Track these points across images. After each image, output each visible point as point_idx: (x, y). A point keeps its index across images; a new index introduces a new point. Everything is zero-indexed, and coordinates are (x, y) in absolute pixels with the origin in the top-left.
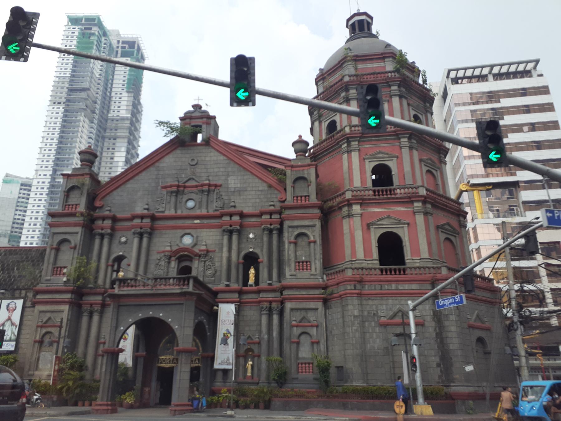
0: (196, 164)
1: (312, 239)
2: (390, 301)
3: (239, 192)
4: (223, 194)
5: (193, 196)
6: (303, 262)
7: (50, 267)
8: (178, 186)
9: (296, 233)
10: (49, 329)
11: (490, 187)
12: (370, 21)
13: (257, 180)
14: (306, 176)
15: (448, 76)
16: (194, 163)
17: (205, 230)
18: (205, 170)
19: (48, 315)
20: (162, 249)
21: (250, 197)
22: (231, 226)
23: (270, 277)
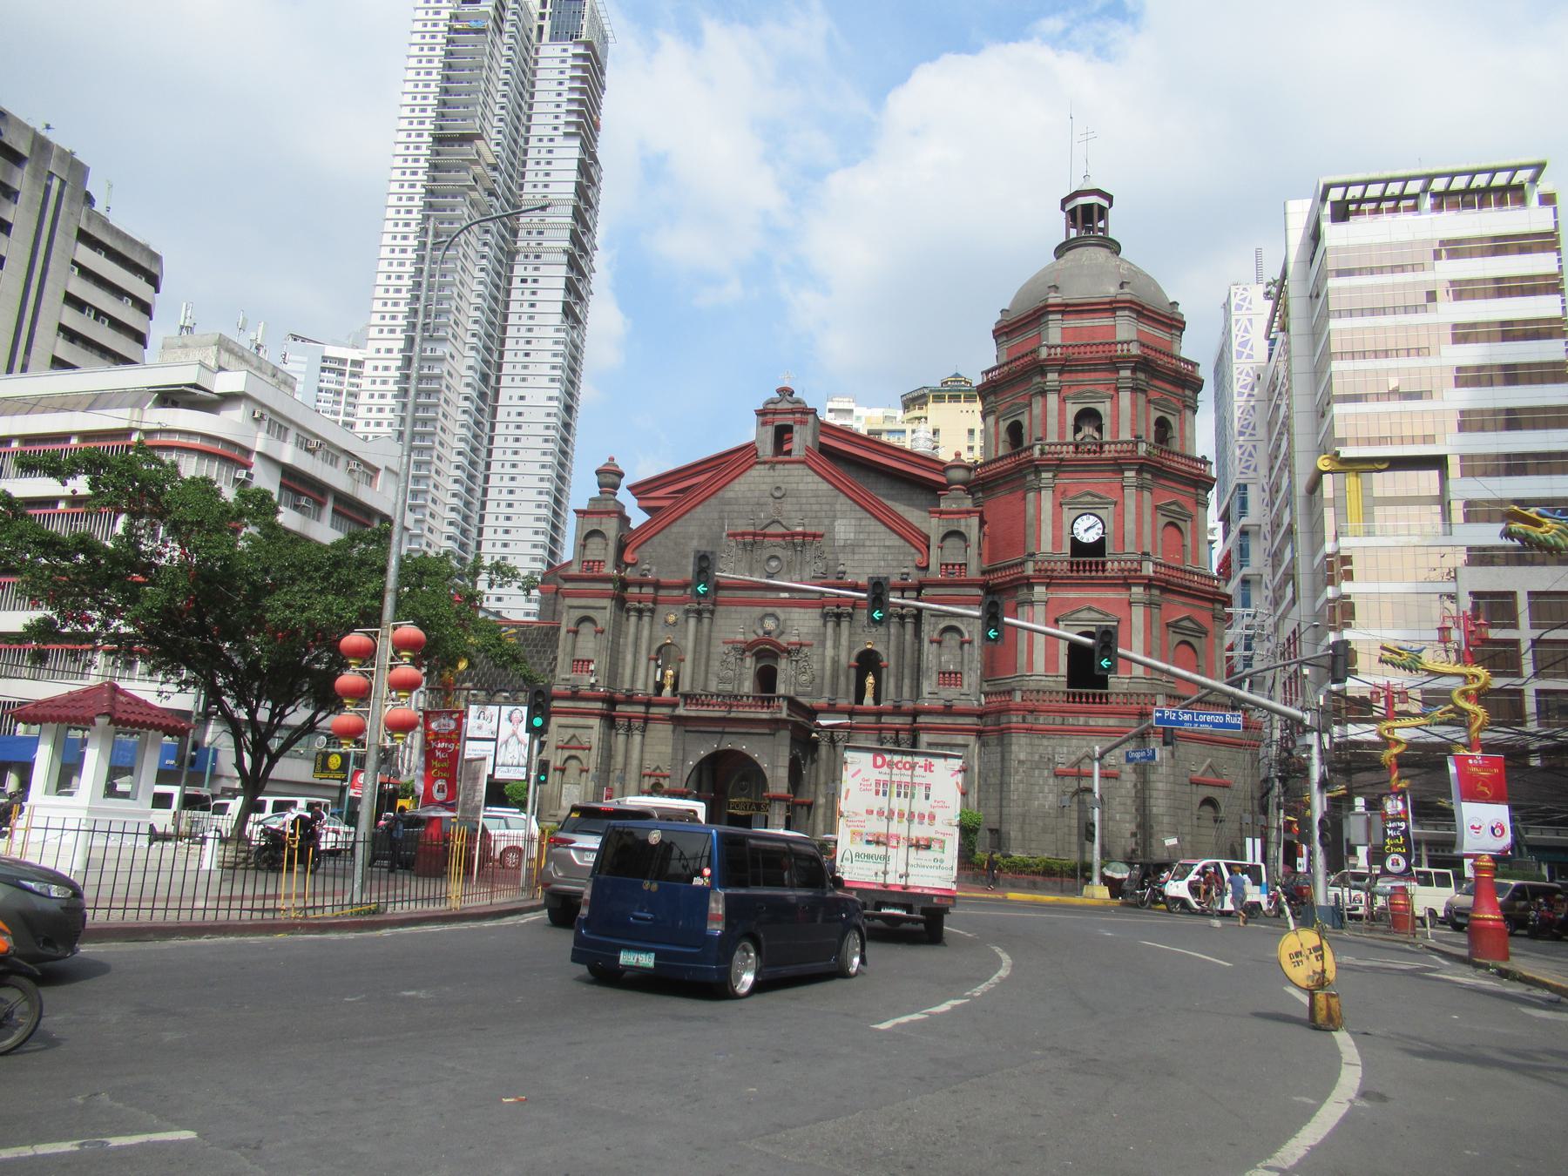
0: (784, 495)
1: (967, 636)
2: (1074, 742)
3: (852, 547)
4: (827, 549)
5: (779, 552)
6: (950, 673)
7: (568, 660)
8: (754, 535)
9: (941, 626)
10: (573, 752)
11: (1385, 466)
12: (1105, 203)
13: (883, 528)
14: (963, 529)
15: (1324, 198)
16: (777, 494)
17: (797, 610)
18: (797, 507)
19: (571, 732)
20: (731, 637)
21: (870, 557)
22: (838, 607)
23: (899, 688)
